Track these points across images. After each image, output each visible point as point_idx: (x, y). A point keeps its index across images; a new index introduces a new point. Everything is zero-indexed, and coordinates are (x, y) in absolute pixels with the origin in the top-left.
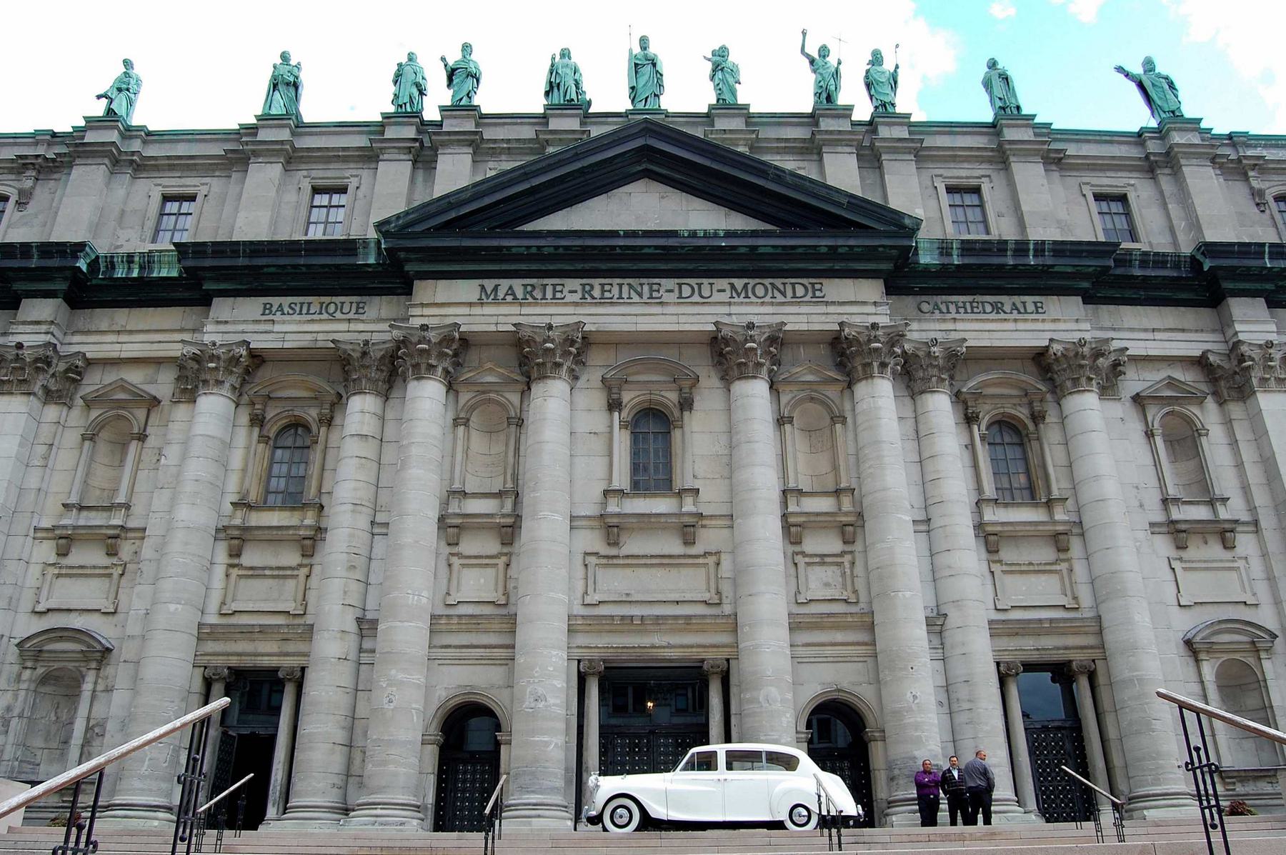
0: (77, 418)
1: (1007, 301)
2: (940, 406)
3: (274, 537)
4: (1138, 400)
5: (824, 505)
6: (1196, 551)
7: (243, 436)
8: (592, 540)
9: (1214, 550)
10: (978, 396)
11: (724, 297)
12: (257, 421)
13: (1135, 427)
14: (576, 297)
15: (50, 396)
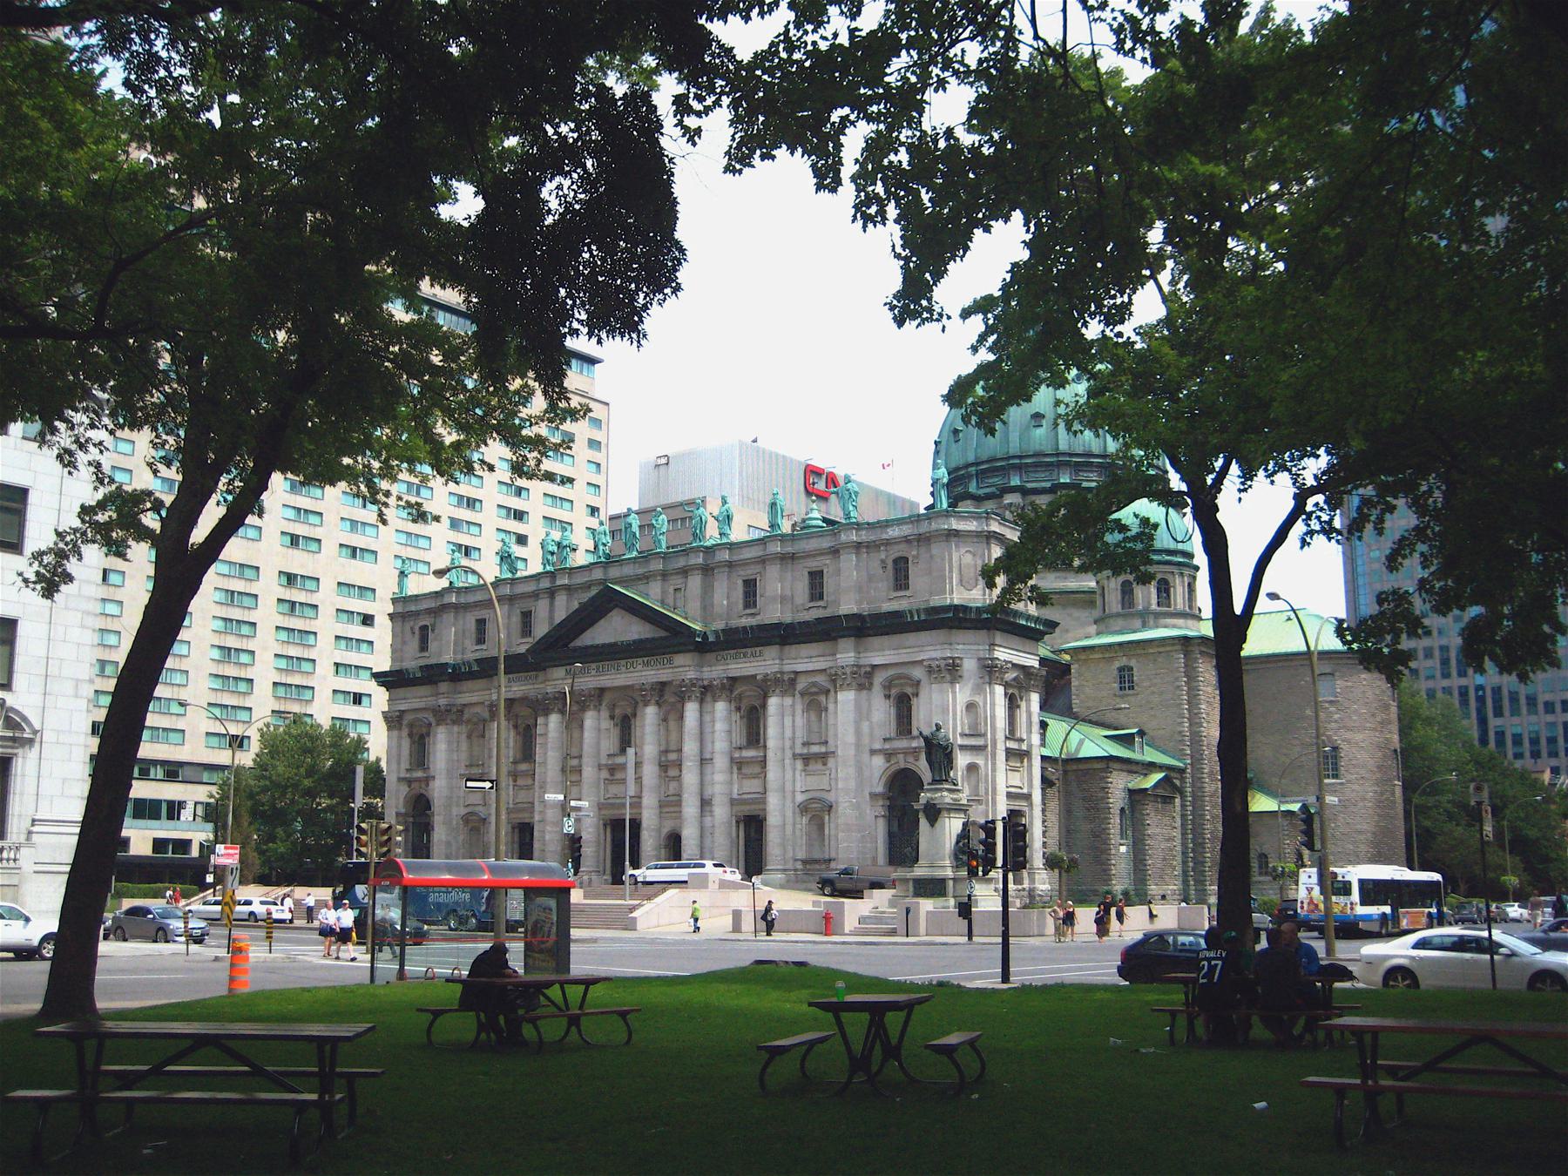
0: (464, 729)
1: (749, 650)
2: (721, 707)
3: (525, 774)
4: (802, 694)
5: (672, 756)
6: (815, 766)
7: (512, 733)
8: (605, 774)
9: (819, 766)
10: (740, 698)
11: (640, 667)
12: (516, 727)
13: (799, 708)
14: (593, 672)
15: (454, 722)
